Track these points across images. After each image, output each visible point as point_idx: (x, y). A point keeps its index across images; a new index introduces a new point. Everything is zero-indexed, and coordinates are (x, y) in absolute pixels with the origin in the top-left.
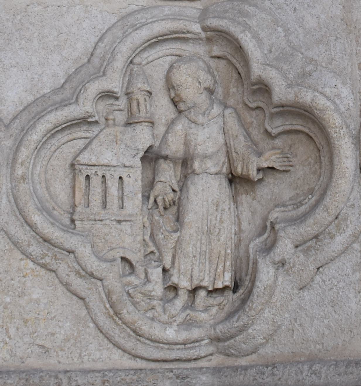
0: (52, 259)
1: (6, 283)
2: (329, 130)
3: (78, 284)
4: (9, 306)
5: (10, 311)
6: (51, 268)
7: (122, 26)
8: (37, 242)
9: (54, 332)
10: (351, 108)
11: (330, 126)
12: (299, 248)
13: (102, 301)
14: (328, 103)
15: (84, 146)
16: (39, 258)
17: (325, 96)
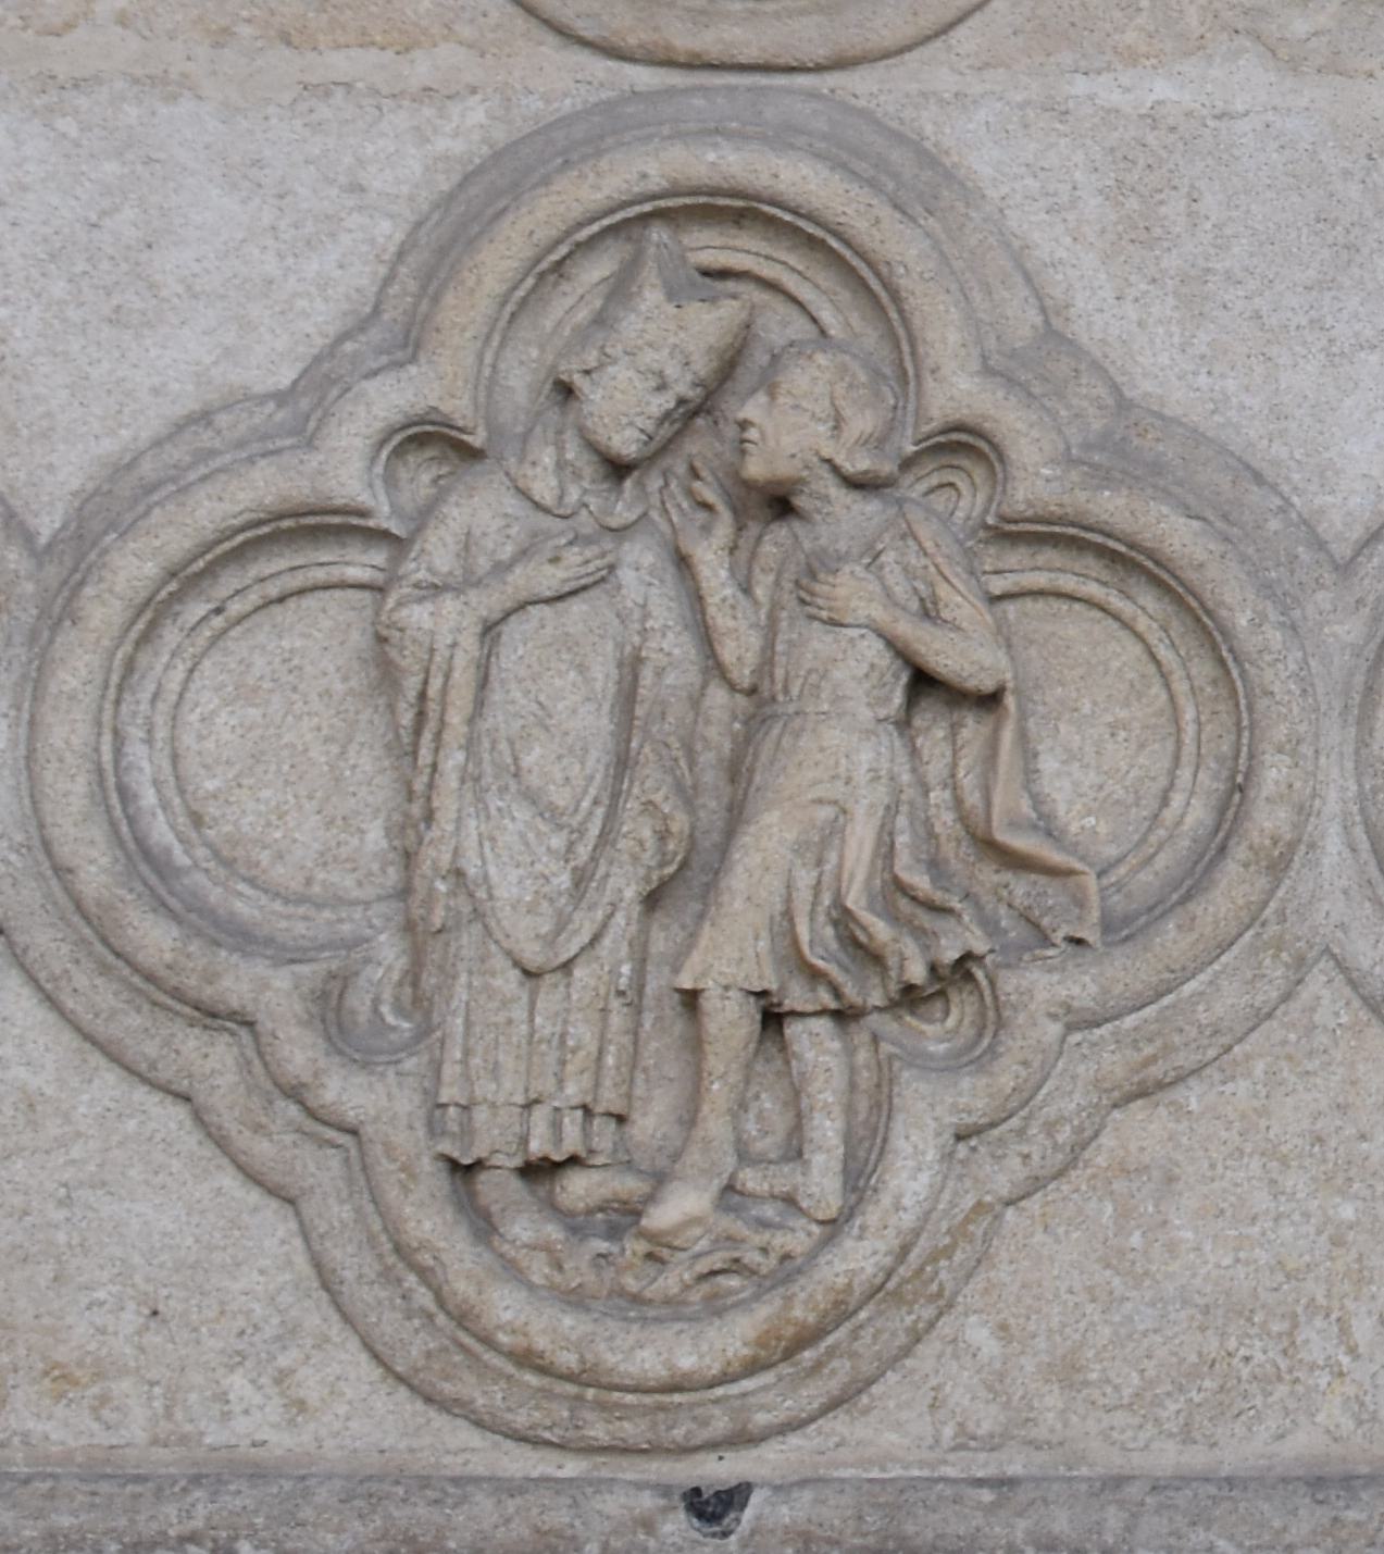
1: (1341, 1149)
4: (1351, 1236)
5: (1354, 1254)
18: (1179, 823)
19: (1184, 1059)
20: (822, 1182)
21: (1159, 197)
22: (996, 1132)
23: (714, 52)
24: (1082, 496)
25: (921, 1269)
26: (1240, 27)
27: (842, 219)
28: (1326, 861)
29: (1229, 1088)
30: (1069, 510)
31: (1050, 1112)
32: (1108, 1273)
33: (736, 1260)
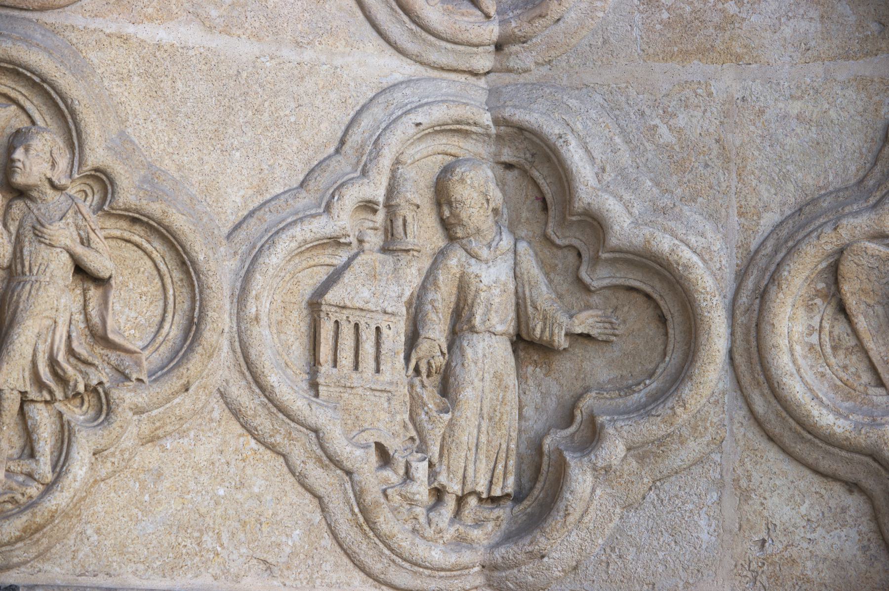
0: (284, 438)
1: (220, 468)
2: (696, 296)
3: (319, 477)
4: (222, 501)
5: (224, 509)
6: (281, 450)
8: (267, 412)
9: (279, 542)
10: (723, 268)
11: (697, 290)
12: (632, 452)
13: (348, 503)
14: (695, 258)
15: (326, 277)
16: (267, 435)
17: (688, 245)
18: (168, 334)
19: (169, 428)
20: (44, 467)
21: (160, 79)
22: (106, 453)
24: (144, 202)
25: (76, 505)
26: (191, 11)
27: (54, 79)
28: (223, 355)
29: (181, 441)
30: (138, 207)
31: (123, 446)
32: (137, 510)
33: (13, 498)
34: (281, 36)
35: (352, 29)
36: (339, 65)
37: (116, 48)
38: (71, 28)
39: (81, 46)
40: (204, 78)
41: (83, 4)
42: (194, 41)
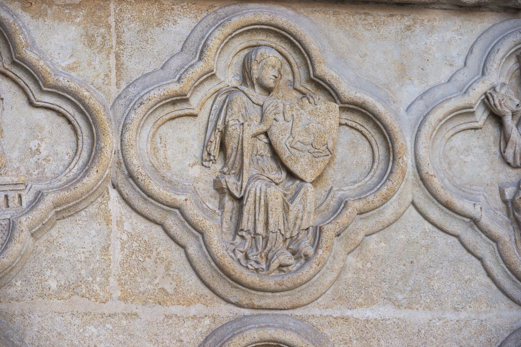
7: (516, 340)
21: (370, 340)
23: (264, 306)
26: (385, 297)
34: (444, 306)
35: (490, 296)
36: (484, 319)
37: (341, 325)
38: (312, 316)
39: (319, 327)
40: (398, 336)
41: (319, 302)
42: (389, 315)
